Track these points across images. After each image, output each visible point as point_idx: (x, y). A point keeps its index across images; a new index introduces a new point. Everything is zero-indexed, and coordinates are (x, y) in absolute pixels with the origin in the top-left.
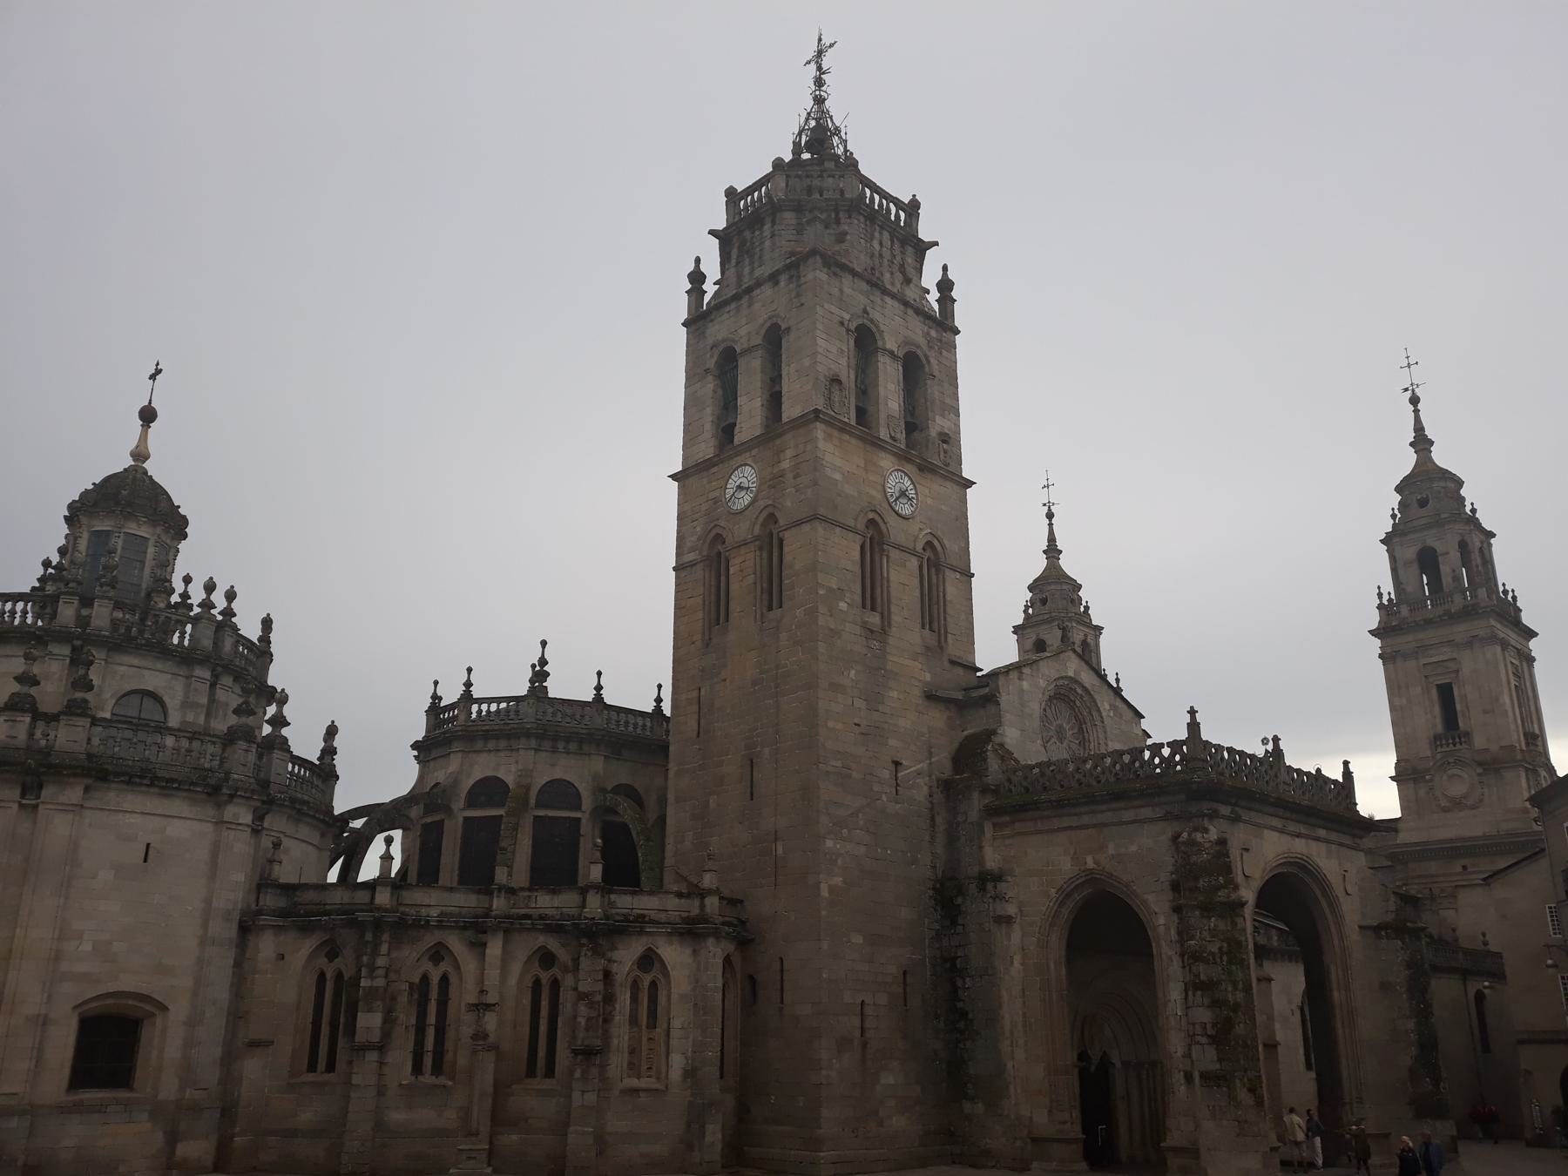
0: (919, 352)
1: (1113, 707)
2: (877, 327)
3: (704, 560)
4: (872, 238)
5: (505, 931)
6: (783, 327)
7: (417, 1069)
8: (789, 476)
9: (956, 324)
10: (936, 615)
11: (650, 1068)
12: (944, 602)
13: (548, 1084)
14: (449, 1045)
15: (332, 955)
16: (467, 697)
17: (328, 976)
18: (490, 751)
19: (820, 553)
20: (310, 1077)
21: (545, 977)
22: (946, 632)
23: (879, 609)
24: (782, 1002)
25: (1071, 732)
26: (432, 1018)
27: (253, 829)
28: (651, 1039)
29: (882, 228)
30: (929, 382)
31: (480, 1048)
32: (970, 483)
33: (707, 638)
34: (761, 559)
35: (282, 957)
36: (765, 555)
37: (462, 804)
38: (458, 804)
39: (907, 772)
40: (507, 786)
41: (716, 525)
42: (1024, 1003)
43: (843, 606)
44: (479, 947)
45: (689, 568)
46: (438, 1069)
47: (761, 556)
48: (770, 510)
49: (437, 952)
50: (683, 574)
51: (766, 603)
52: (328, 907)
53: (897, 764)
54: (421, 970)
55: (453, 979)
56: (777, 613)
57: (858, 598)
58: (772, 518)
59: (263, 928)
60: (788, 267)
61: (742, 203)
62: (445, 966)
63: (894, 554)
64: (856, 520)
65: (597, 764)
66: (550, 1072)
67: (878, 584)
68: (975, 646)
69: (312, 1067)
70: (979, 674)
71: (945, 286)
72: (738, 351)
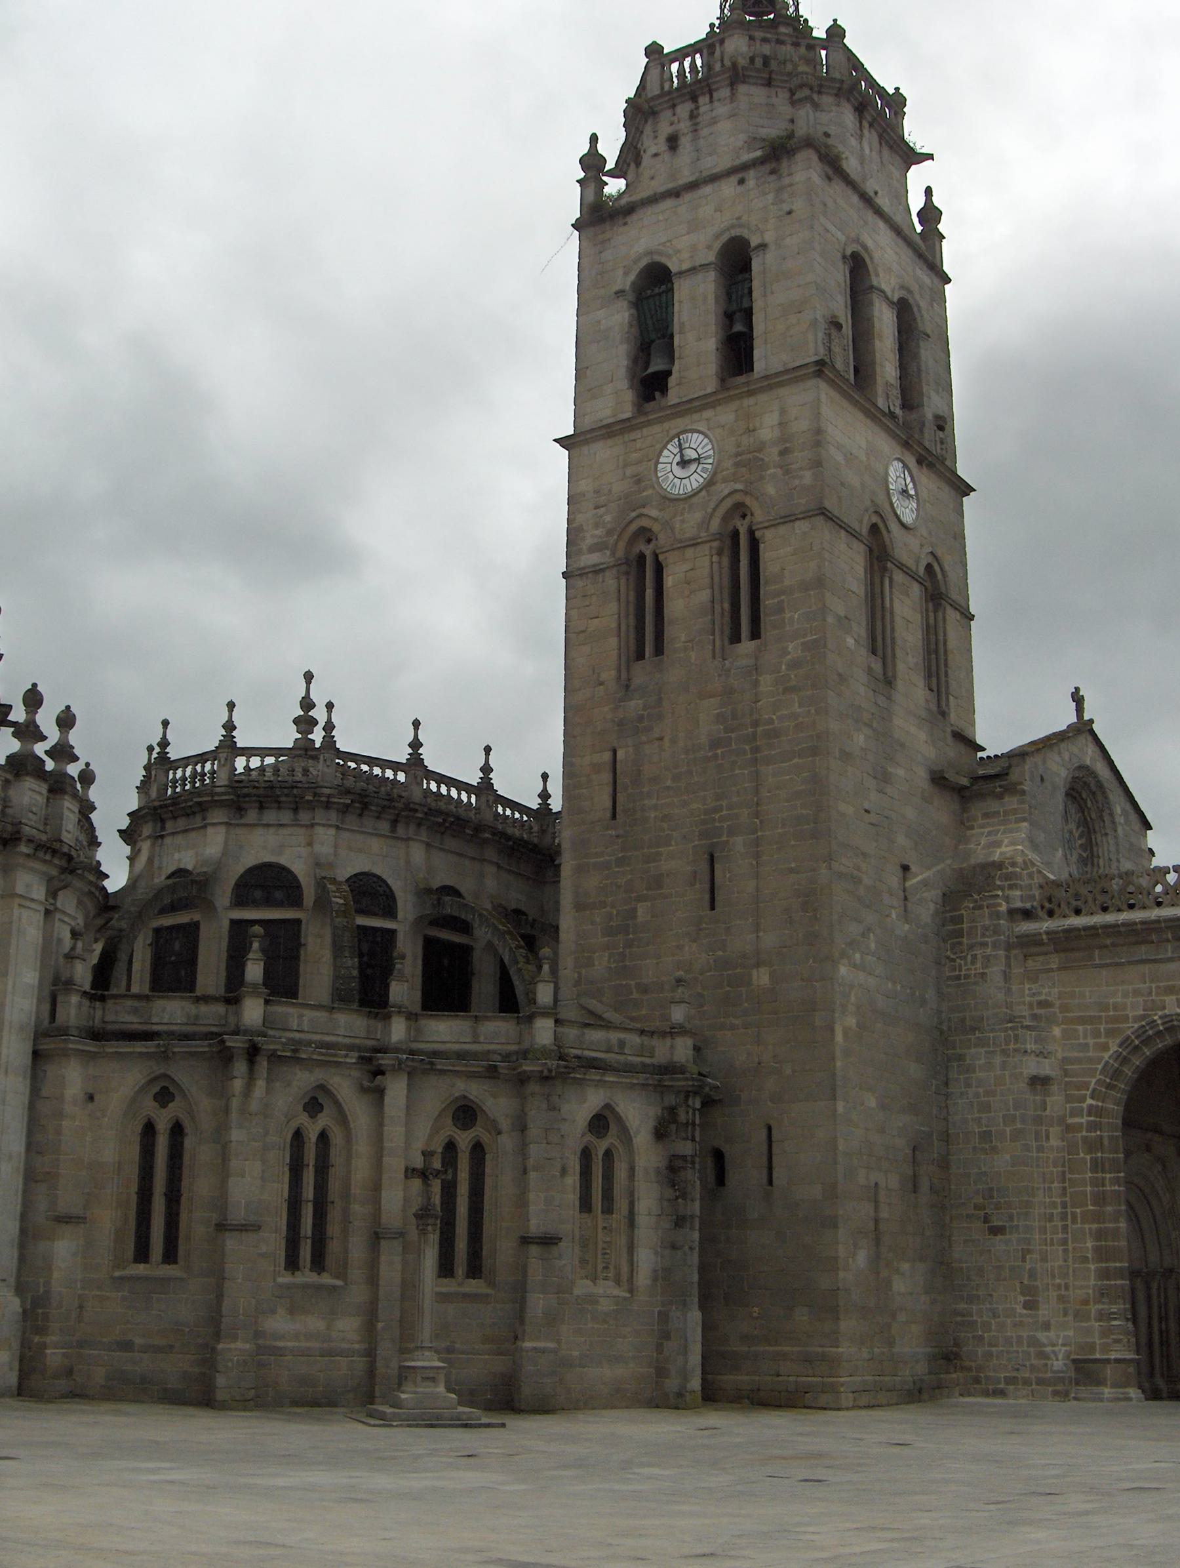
0: (911, 301)
1: (1124, 811)
2: (871, 258)
3: (619, 565)
4: (861, 136)
5: (409, 1073)
6: (754, 241)
7: (292, 1263)
8: (772, 454)
9: (945, 268)
10: (934, 668)
11: (606, 1268)
12: (946, 652)
13: (474, 1286)
14: (333, 1229)
15: (164, 1097)
16: (229, 747)
17: (163, 1127)
18: (268, 825)
19: (826, 564)
20: (141, 1269)
21: (464, 1140)
22: (947, 694)
23: (880, 653)
24: (770, 1183)
25: (1080, 842)
26: (309, 1192)
27: (46, 909)
28: (605, 1228)
29: (871, 125)
30: (922, 344)
32: (966, 489)
33: (624, 675)
34: (721, 568)
35: (91, 1098)
36: (726, 561)
37: (227, 902)
38: (223, 896)
39: (915, 881)
40: (295, 877)
41: (640, 516)
42: (1064, 1189)
43: (850, 641)
45: (590, 575)
46: (318, 1263)
47: (720, 563)
48: (738, 498)
50: (580, 583)
51: (727, 631)
52: (156, 1028)
53: (906, 868)
54: (294, 1125)
56: (747, 646)
57: (863, 632)
58: (741, 510)
59: (65, 1054)
60: (762, 161)
61: (675, 67)
62: (324, 1120)
63: (899, 577)
64: (861, 522)
65: (418, 853)
66: (475, 1269)
67: (878, 615)
68: (976, 716)
69: (142, 1254)
70: (980, 754)
71: (930, 214)
72: (674, 268)
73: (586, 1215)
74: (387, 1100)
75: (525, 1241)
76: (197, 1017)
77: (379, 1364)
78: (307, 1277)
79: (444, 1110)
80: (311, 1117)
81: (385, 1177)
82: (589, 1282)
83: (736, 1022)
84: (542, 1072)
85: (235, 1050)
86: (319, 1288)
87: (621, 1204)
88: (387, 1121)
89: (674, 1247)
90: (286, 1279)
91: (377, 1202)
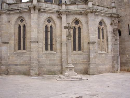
5: (66, 15)
7: (46, 49)
11: (103, 49)
13: (80, 52)
14: (54, 43)
15: (22, 21)
17: (21, 26)
20: (19, 51)
26: (49, 36)
28: (102, 42)
31: (70, 39)
44: (60, 18)
46: (51, 49)
49: (49, 20)
55: (54, 27)
62: (51, 24)
66: (80, 49)
69: (19, 49)
73: (99, 39)
74: (62, 19)
75: (89, 43)
76: (26, 6)
77: (63, 67)
78: (49, 51)
79: (73, 21)
80: (49, 23)
81: (63, 33)
82: (100, 51)
83: (121, 8)
84: (90, 11)
85: (31, 8)
86: (51, 53)
87: (105, 37)
88: (62, 23)
89: (115, 45)
90: (45, 52)
91: (61, 38)
